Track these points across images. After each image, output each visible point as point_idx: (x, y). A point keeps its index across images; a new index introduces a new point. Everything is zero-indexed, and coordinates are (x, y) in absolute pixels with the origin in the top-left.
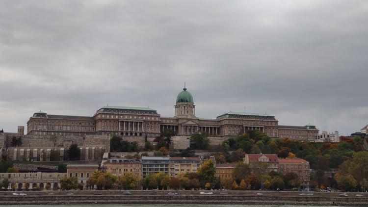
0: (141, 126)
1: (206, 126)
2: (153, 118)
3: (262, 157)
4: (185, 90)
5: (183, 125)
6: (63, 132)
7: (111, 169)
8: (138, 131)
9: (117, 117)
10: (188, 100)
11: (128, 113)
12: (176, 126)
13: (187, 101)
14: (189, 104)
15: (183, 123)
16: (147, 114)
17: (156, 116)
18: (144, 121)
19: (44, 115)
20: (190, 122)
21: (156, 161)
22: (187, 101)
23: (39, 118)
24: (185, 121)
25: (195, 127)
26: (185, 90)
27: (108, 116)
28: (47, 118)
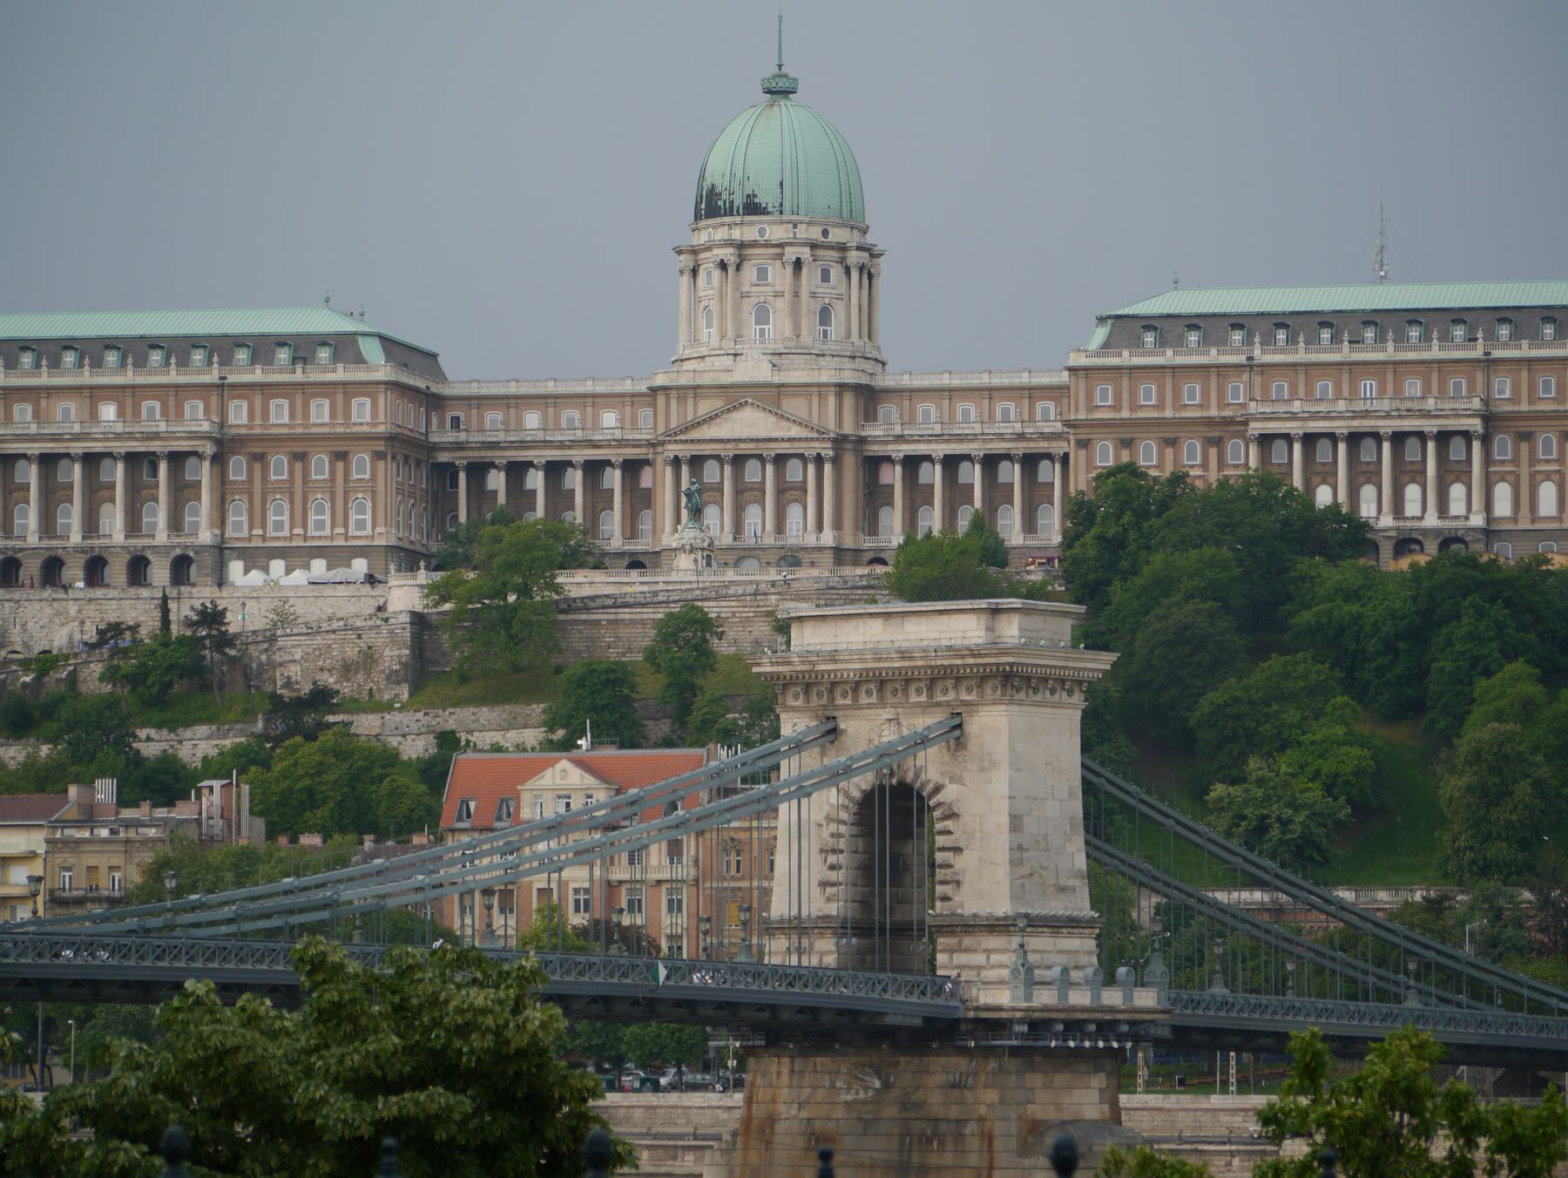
0: (183, 492)
1: (940, 450)
2: (320, 413)
3: (548, 778)
5: (673, 449)
8: (162, 537)
10: (762, 199)
11: (87, 377)
12: (632, 468)
13: (753, 208)
14: (777, 233)
15: (672, 435)
16: (258, 375)
20: (750, 424)
22: (753, 208)
24: (705, 407)
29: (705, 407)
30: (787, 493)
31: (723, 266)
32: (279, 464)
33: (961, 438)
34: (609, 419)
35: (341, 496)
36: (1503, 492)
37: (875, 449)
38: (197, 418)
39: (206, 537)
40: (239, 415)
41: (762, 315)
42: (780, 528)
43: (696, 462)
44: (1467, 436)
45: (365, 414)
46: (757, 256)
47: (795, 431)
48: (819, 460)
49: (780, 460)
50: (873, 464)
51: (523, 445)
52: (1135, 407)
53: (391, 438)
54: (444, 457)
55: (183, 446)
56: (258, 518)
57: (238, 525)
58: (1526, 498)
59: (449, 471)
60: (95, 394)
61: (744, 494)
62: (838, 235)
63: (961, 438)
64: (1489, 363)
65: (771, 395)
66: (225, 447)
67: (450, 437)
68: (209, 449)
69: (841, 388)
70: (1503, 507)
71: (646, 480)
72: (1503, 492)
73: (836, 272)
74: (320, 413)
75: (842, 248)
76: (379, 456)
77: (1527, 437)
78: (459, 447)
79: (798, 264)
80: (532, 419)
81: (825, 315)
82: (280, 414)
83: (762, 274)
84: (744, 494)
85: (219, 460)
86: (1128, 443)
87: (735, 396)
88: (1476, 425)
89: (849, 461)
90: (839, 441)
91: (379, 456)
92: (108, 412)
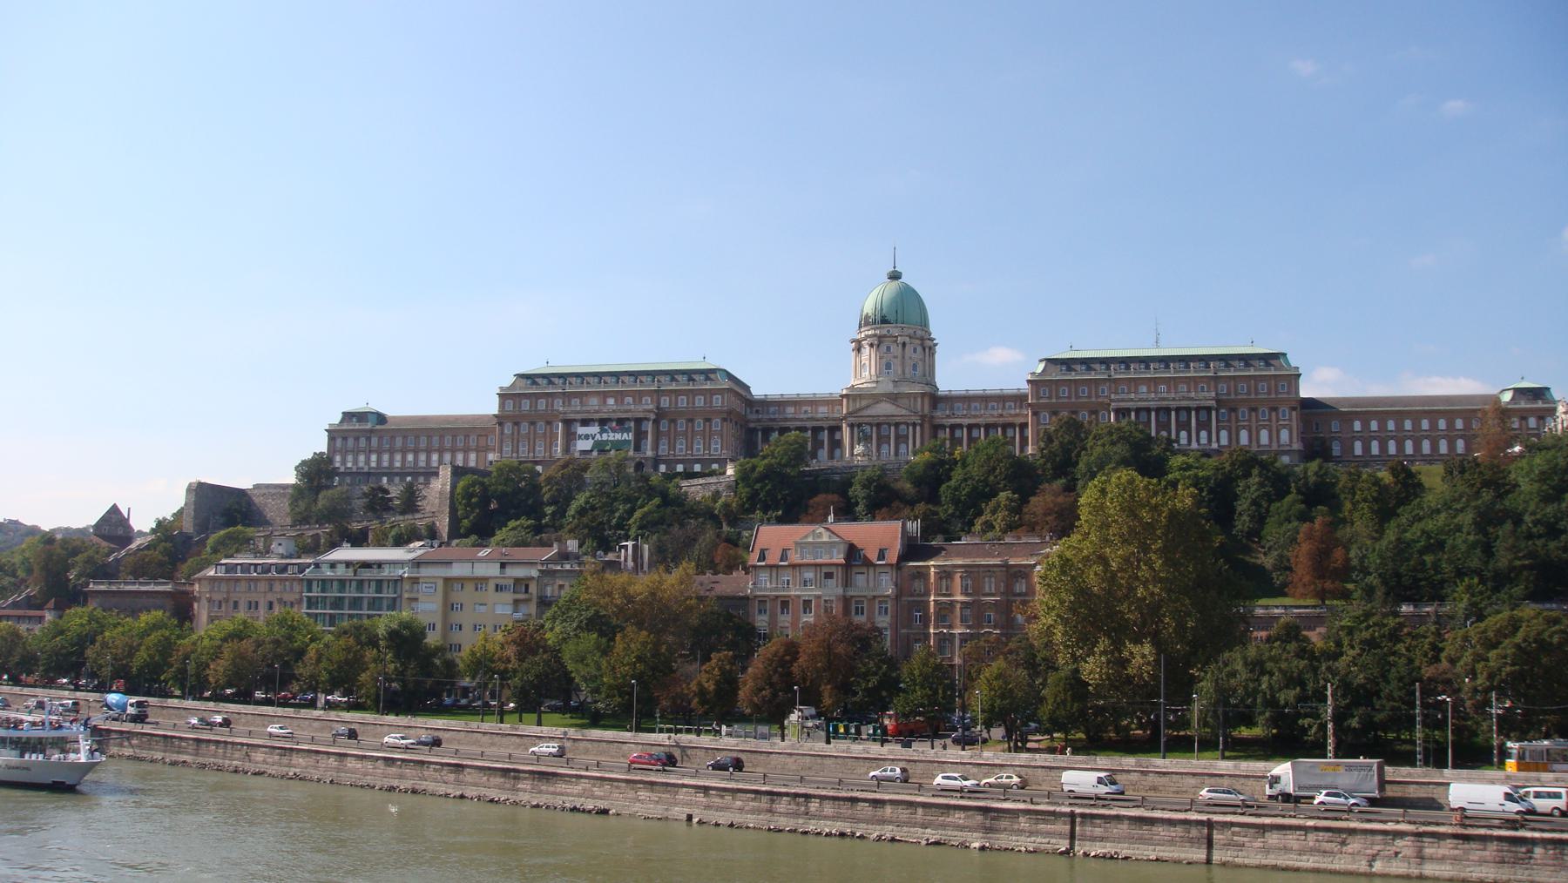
1: (966, 421)
2: (700, 401)
4: (895, 276)
6: (415, 475)
7: (209, 600)
9: (558, 405)
10: (890, 317)
13: (884, 321)
16: (674, 387)
17: (712, 392)
18: (660, 414)
19: (361, 416)
20: (885, 408)
21: (366, 565)
23: (345, 427)
25: (907, 425)
26: (895, 276)
27: (526, 405)
28: (369, 426)
29: (864, 403)
30: (901, 439)
31: (871, 345)
32: (681, 425)
33: (975, 416)
34: (823, 409)
35: (707, 437)
36: (1224, 434)
37: (938, 422)
38: (648, 404)
39: (649, 453)
40: (665, 402)
41: (888, 366)
42: (896, 454)
43: (859, 425)
44: (1209, 409)
45: (718, 401)
46: (887, 342)
47: (904, 412)
48: (914, 425)
49: (897, 425)
50: (936, 428)
51: (786, 420)
52: (1058, 397)
53: (730, 412)
54: (752, 425)
55: (641, 415)
56: (672, 446)
57: (663, 449)
58: (1233, 437)
59: (755, 430)
60: (605, 395)
61: (883, 440)
62: (919, 333)
63: (975, 416)
64: (1216, 379)
65: (893, 398)
66: (660, 414)
67: (754, 416)
68: (653, 416)
69: (923, 395)
70: (1224, 441)
71: (837, 436)
72: (1224, 434)
73: (919, 349)
74: (700, 401)
75: (922, 339)
76: (724, 420)
77: (1234, 410)
78: (759, 420)
79: (904, 344)
80: (790, 410)
81: (915, 367)
82: (683, 402)
83: (888, 348)
84: (883, 440)
85: (656, 422)
86: (1055, 413)
87: (876, 398)
88: (1213, 403)
89: (927, 426)
90: (923, 417)
91: (724, 420)
92: (611, 401)
